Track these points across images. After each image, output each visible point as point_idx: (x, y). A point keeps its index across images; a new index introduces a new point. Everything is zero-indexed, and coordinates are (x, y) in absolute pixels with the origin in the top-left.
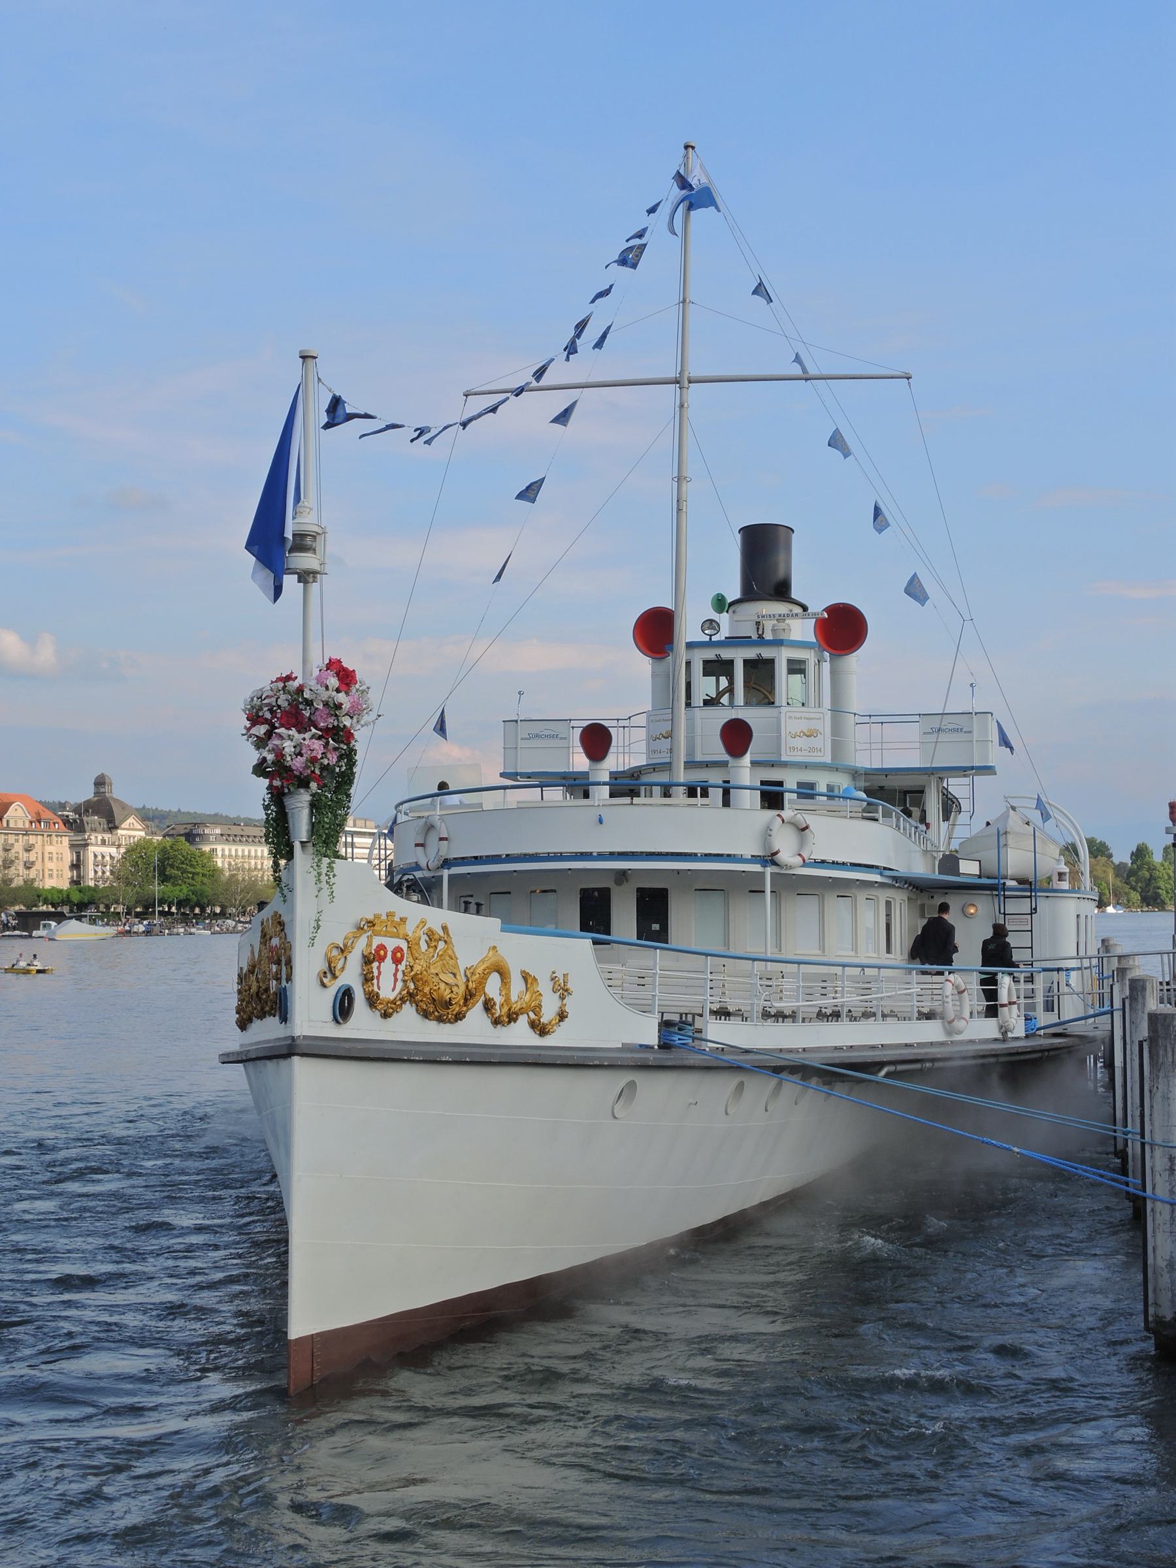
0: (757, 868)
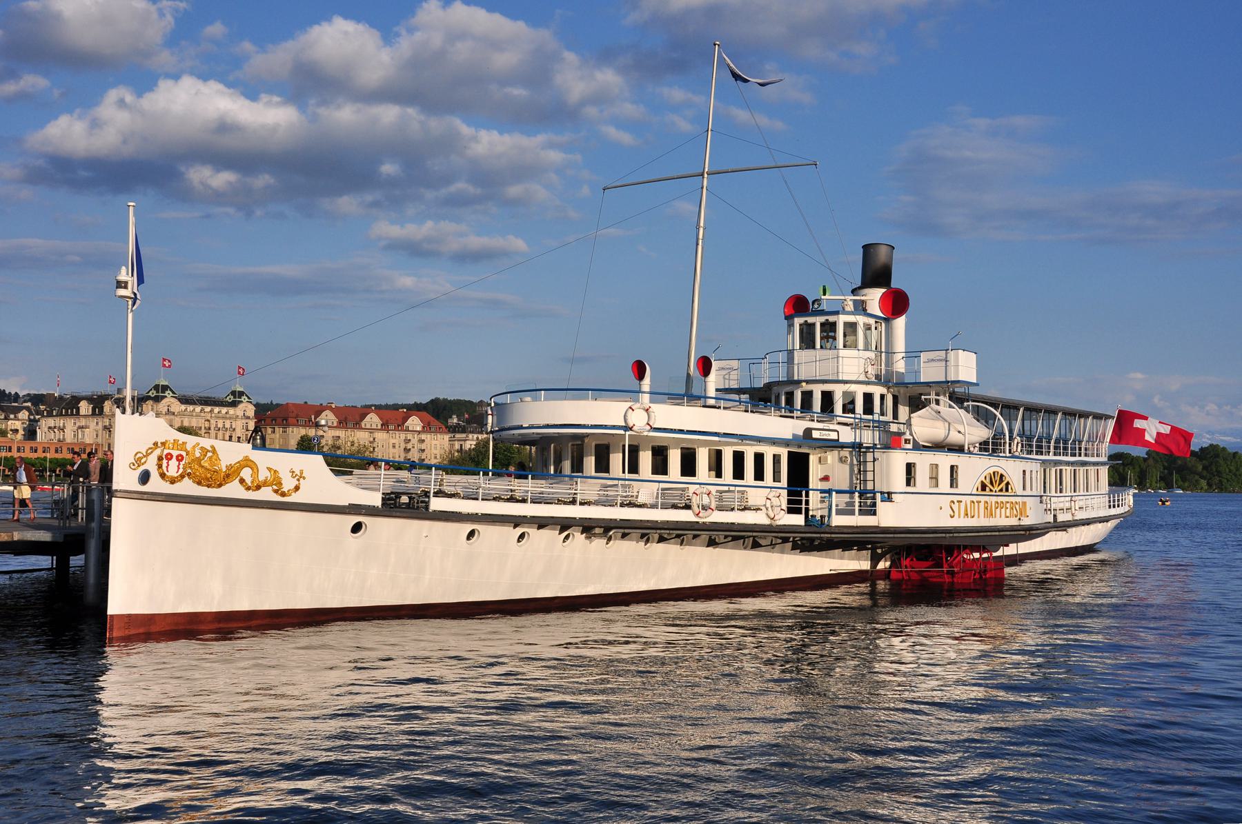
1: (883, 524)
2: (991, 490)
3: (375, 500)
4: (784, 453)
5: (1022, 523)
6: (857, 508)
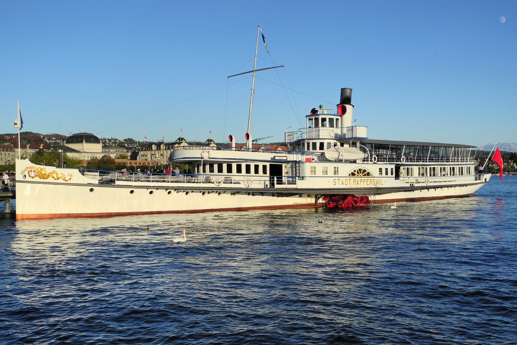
0: (200, 159)
1: (299, 187)
2: (358, 175)
3: (97, 182)
4: (268, 165)
5: (377, 187)
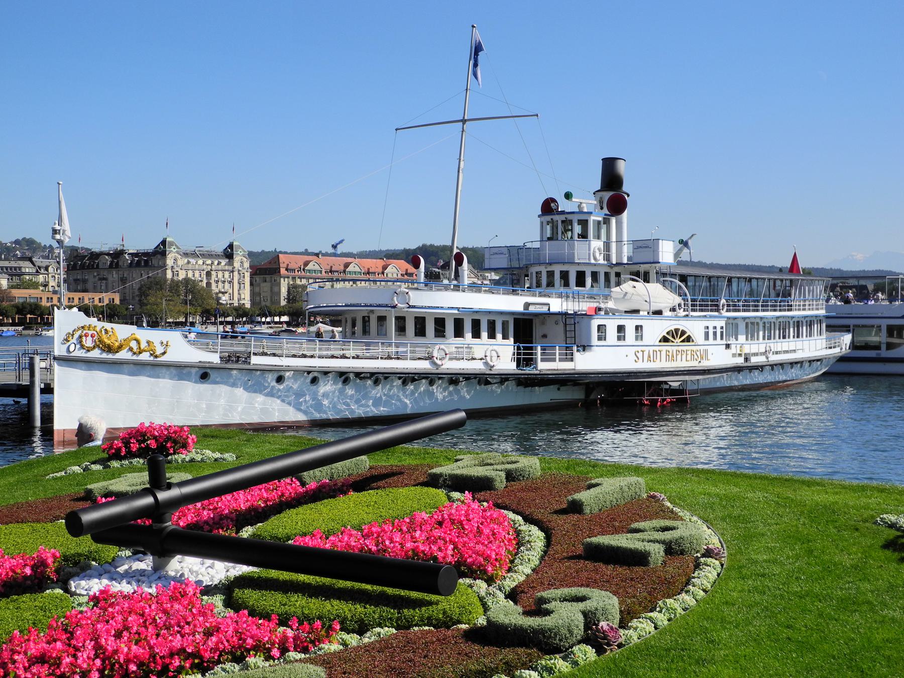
2: (673, 342)
5: (701, 364)
6: (557, 357)
